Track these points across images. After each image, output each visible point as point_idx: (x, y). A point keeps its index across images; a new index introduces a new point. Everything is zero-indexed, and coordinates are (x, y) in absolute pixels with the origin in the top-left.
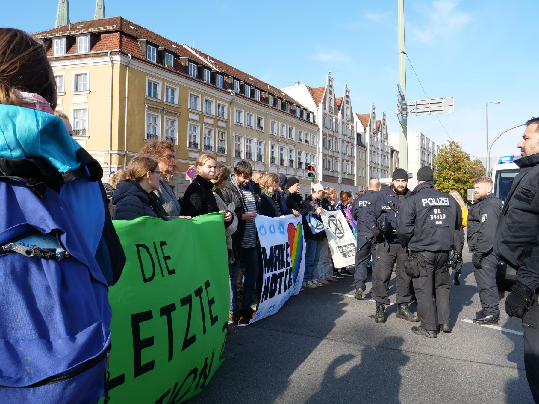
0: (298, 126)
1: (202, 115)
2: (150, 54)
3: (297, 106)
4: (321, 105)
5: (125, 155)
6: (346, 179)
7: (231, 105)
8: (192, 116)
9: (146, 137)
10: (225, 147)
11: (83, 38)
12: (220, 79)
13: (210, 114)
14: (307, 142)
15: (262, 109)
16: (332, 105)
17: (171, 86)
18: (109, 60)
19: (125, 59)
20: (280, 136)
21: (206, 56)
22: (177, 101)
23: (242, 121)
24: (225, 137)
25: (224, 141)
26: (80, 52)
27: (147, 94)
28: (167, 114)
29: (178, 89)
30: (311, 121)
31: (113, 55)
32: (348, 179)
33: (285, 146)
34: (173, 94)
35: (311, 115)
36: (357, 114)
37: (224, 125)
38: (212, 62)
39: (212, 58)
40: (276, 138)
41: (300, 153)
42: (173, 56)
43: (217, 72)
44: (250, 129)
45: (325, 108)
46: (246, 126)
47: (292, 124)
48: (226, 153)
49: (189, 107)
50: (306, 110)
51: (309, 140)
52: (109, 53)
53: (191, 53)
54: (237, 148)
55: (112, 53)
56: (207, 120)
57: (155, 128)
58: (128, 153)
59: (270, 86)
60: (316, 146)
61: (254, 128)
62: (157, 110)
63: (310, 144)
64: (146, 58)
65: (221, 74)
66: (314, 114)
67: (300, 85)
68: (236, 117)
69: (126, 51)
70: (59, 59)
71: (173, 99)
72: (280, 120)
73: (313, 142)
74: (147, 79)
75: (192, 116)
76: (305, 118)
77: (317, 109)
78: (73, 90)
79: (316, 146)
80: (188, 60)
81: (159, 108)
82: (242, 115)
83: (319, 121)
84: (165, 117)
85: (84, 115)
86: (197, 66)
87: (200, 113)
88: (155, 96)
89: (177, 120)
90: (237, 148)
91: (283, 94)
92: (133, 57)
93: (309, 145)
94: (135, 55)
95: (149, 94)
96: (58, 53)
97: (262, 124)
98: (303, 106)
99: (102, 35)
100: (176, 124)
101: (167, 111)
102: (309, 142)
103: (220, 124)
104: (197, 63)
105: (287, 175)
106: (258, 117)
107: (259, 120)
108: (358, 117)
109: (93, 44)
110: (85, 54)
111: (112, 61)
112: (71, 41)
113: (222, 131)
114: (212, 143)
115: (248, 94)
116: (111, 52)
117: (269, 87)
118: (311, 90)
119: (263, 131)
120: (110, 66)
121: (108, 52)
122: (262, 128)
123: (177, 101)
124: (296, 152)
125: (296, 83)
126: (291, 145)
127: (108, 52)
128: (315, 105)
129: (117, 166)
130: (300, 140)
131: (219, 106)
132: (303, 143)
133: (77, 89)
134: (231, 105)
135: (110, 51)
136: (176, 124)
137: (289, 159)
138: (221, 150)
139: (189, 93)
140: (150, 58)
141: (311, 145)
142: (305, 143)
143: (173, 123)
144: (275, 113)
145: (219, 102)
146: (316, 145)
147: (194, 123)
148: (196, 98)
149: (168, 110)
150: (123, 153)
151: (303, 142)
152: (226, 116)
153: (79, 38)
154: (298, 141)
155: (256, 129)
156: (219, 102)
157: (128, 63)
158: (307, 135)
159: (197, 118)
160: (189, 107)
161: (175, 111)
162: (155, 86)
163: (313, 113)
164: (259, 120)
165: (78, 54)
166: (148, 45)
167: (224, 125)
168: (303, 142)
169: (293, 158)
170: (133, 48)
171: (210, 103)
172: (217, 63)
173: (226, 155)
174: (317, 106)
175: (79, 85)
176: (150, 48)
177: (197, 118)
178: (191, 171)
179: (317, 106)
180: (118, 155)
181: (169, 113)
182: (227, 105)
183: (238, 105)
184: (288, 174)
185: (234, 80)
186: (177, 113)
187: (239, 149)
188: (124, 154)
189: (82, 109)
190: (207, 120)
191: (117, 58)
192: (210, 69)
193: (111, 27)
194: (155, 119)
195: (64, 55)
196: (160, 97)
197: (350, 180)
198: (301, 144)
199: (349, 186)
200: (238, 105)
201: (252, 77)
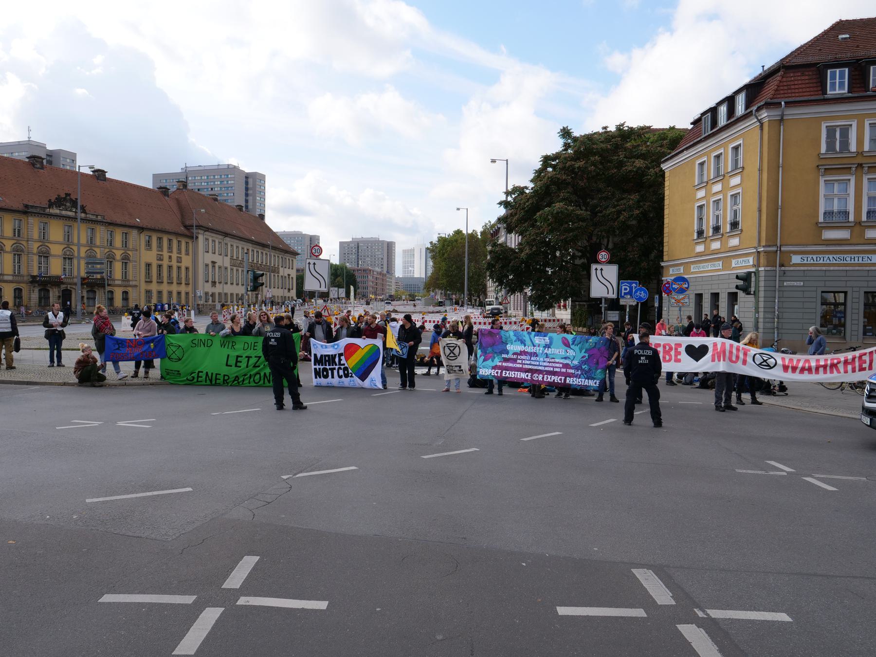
18: (756, 120)
19: (775, 113)
27: (823, 149)
28: (868, 173)
52: (754, 112)
62: (846, 170)
74: (824, 126)
94: (787, 100)
101: (869, 167)
111: (759, 121)
149: (867, 165)
157: (782, 115)
162: (845, 131)
178: (667, 285)
188: (777, 250)
196: (853, 148)
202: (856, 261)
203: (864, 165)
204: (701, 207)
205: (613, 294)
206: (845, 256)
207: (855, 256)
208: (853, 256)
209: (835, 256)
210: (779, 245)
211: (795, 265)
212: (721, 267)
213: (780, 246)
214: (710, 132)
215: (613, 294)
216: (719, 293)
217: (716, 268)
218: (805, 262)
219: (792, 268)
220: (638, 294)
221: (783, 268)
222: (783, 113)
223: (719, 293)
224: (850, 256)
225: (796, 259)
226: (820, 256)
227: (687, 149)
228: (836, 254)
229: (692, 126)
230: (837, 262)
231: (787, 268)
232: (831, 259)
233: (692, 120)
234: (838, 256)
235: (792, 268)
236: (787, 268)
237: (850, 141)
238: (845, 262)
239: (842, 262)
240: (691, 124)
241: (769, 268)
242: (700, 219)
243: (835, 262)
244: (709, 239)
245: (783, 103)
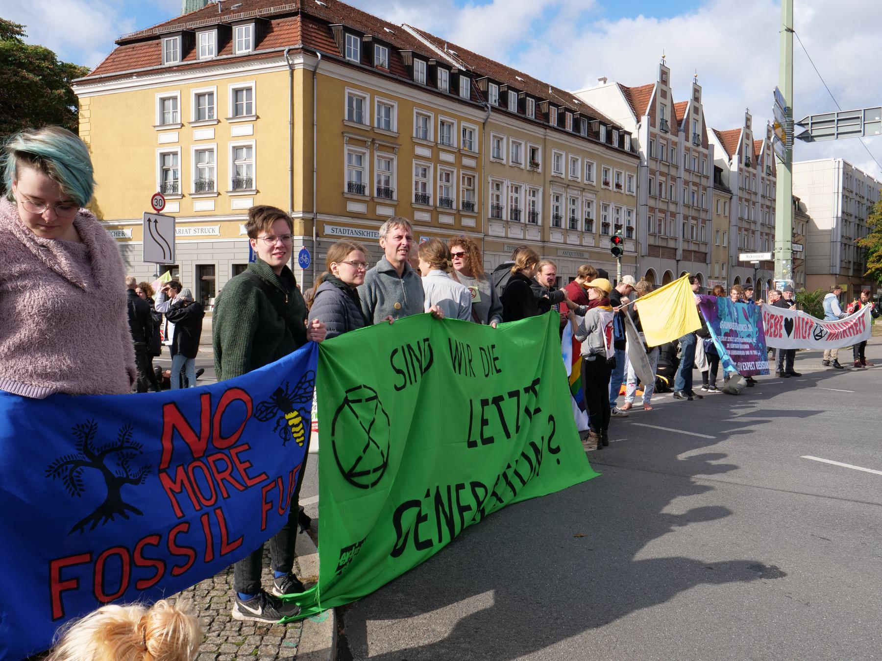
0: (601, 160)
1: (436, 149)
2: (350, 49)
3: (601, 123)
4: (645, 119)
5: (315, 220)
6: (691, 251)
7: (484, 128)
8: (419, 151)
9: (346, 190)
10: (476, 200)
11: (243, 27)
12: (464, 83)
13: (449, 146)
14: (618, 186)
15: (539, 132)
16: (668, 117)
17: (385, 102)
18: (286, 63)
19: (311, 61)
20: (570, 178)
21: (440, 43)
22: (395, 127)
23: (504, 155)
24: (474, 183)
25: (474, 190)
26: (239, 52)
29: (396, 105)
30: (627, 147)
31: (293, 54)
32: (695, 252)
33: (578, 195)
34: (388, 115)
35: (627, 138)
36: (715, 131)
37: (471, 163)
38: (452, 52)
39: (451, 46)
40: (562, 181)
41: (606, 207)
42: (387, 50)
43: (460, 71)
44: (516, 169)
45: (652, 124)
46: (511, 163)
47: (591, 155)
48: (476, 209)
49: (414, 135)
50: (618, 128)
51: (622, 183)
53: (416, 39)
54: (495, 202)
55: (291, 52)
56: (444, 156)
57: (359, 174)
58: (320, 217)
59: (553, 88)
60: (634, 194)
61: (523, 166)
62: (363, 143)
63: (624, 190)
64: (344, 57)
65: (467, 74)
66: (633, 137)
67: (606, 85)
68: (494, 148)
69: (311, 47)
70: (210, 63)
71: (388, 123)
72: (569, 150)
73: (630, 186)
74: (347, 91)
75: (419, 151)
76: (616, 145)
77: (638, 126)
78: (230, 116)
79: (634, 194)
80: (411, 54)
81: (366, 139)
82: (504, 143)
83: (643, 149)
84: (376, 154)
85: (249, 156)
86: (427, 64)
87: (433, 144)
88: (360, 120)
89: (395, 158)
90: (495, 202)
91: (576, 102)
92: (322, 56)
93: (622, 191)
94: (330, 53)
95: (350, 118)
96: (206, 55)
97: (539, 159)
98: (612, 123)
99: (273, 22)
100: (395, 162)
101: (379, 145)
102: (623, 187)
103: (466, 161)
104: (425, 59)
105: (582, 246)
106: (530, 147)
107: (534, 151)
108: (717, 135)
109: (259, 39)
110: (248, 54)
112: (225, 37)
113: (469, 173)
114: (453, 196)
115: (513, 107)
116: (289, 50)
117: (550, 91)
118: (627, 93)
119: (540, 170)
120: (288, 73)
121: (283, 51)
122: (537, 165)
123: (395, 127)
124: (598, 205)
125: (600, 80)
126: (590, 193)
127: (283, 51)
128: (633, 120)
129: (301, 237)
130: (606, 183)
131: (464, 130)
132: (611, 188)
133: (237, 111)
134: (484, 128)
135: (287, 49)
136: (395, 162)
137: (586, 219)
138: (468, 206)
139: (415, 111)
140: (350, 56)
141: (627, 193)
142: (615, 190)
143: (389, 163)
144: (562, 138)
145: (464, 124)
146: (635, 191)
147: (422, 163)
148: (427, 119)
149: (379, 142)
150: (310, 216)
151: (612, 186)
152: (476, 148)
153: (237, 29)
154: (603, 186)
155: (528, 168)
156: (464, 124)
157: (316, 68)
158: (619, 174)
159: (426, 152)
160: (414, 135)
161: (392, 143)
162: (360, 102)
163: (630, 134)
164: (534, 151)
165: (237, 56)
166: (347, 34)
167: (471, 163)
168: (612, 186)
169: (593, 217)
170: (323, 41)
171: (450, 125)
172: (461, 54)
173: (476, 215)
174: (638, 121)
175: (239, 107)
176: (350, 38)
177: (426, 152)
179: (638, 121)
180: (303, 219)
181: (382, 147)
182: (476, 128)
183: (496, 127)
184: (584, 244)
185: (490, 84)
186: (394, 146)
187: (498, 204)
189: (244, 146)
190: (444, 156)
191: (299, 60)
192: (448, 67)
193: (287, 6)
194: (360, 158)
195: (215, 58)
196: (367, 120)
197: (698, 252)
198: (608, 191)
199: (697, 263)
200: (496, 127)
201: (521, 75)
202: (371, 237)
203: (376, 142)
204: (164, 156)
205: (171, 259)
206: (364, 230)
207: (371, 231)
208: (369, 231)
209: (356, 230)
210: (315, 212)
211: (328, 236)
212: (217, 233)
213: (317, 213)
214: (178, 62)
215: (171, 259)
216: (213, 266)
217: (203, 234)
218: (335, 234)
219: (325, 240)
220: (302, 258)
221: (318, 239)
222: (317, 65)
223: (213, 266)
224: (367, 230)
225: (328, 230)
226: (346, 228)
227: (139, 74)
228: (357, 228)
229: (117, 46)
230: (358, 236)
231: (322, 239)
232: (354, 232)
233: (117, 38)
234: (359, 230)
235: (325, 240)
236: (322, 239)
237: (363, 113)
238: (363, 237)
239: (361, 236)
240: (118, 43)
241: (307, 238)
242: (164, 170)
243: (356, 236)
244: (188, 198)
245: (319, 55)
